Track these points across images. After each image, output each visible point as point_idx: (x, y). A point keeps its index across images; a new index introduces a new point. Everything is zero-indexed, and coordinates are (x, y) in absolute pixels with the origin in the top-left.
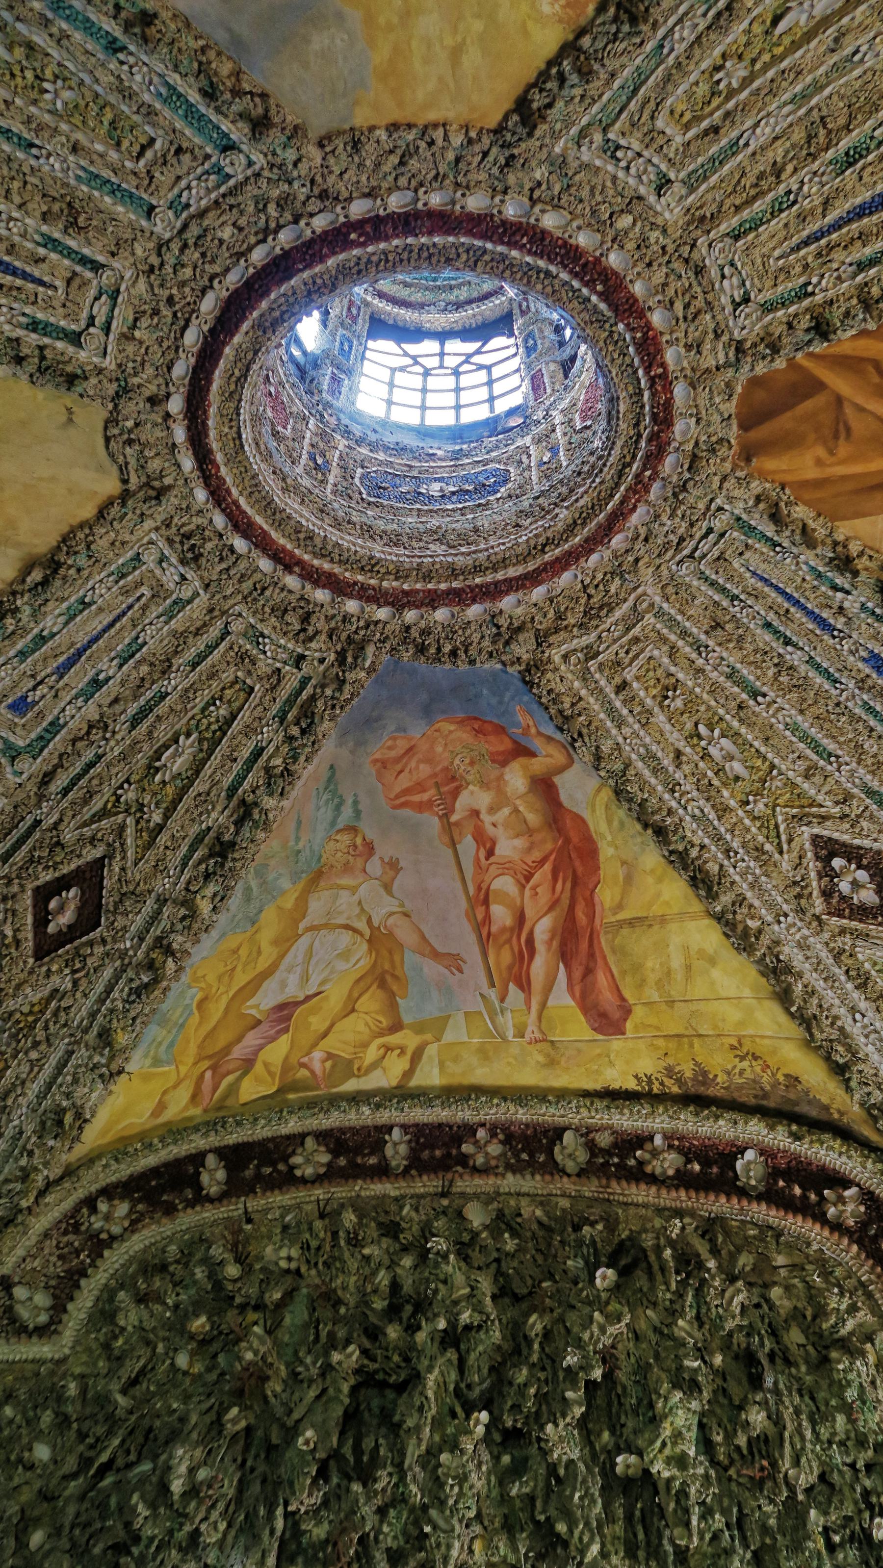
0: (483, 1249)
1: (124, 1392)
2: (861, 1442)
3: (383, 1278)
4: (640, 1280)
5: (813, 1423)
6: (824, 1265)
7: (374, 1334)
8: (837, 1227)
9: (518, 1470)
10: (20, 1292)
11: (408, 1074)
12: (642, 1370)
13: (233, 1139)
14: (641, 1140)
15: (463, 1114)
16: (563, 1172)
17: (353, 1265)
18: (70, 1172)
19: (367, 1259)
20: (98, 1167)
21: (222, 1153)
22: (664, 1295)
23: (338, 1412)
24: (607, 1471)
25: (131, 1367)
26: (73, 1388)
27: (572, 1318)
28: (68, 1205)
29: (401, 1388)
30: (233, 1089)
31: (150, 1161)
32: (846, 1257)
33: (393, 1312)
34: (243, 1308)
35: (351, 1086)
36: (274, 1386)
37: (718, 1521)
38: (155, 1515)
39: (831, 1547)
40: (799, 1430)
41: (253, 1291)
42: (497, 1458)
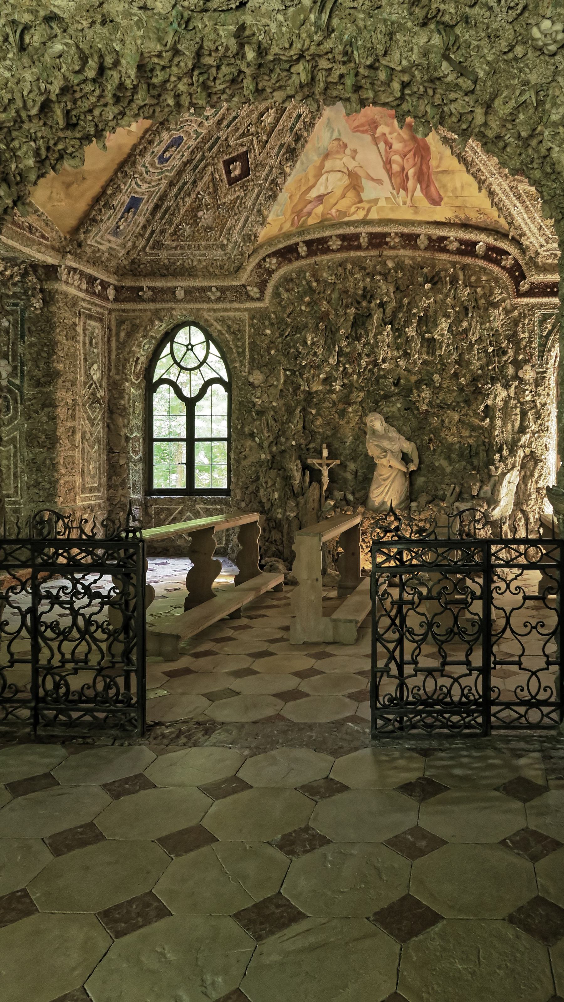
0: (392, 276)
1: (288, 317)
2: (492, 329)
3: (361, 284)
4: (439, 286)
5: (481, 324)
6: (497, 280)
7: (359, 303)
8: (504, 268)
9: (399, 337)
10: (249, 288)
11: (367, 214)
12: (436, 312)
13: (308, 238)
14: (445, 238)
15: (386, 230)
16: (419, 249)
17: (352, 280)
18: (255, 251)
19: (356, 278)
20: (264, 249)
21: (304, 242)
22: (445, 291)
23: (350, 324)
24: (423, 338)
25: (289, 311)
26: (273, 316)
27: (417, 298)
28: (257, 261)
29: (367, 317)
30: (306, 221)
31: (281, 246)
32: (504, 278)
33: (364, 297)
34: (319, 293)
35: (346, 219)
36: (332, 316)
37: (451, 347)
38: (304, 349)
39: (478, 353)
40: (476, 328)
41: (322, 289)
42: (394, 333)
